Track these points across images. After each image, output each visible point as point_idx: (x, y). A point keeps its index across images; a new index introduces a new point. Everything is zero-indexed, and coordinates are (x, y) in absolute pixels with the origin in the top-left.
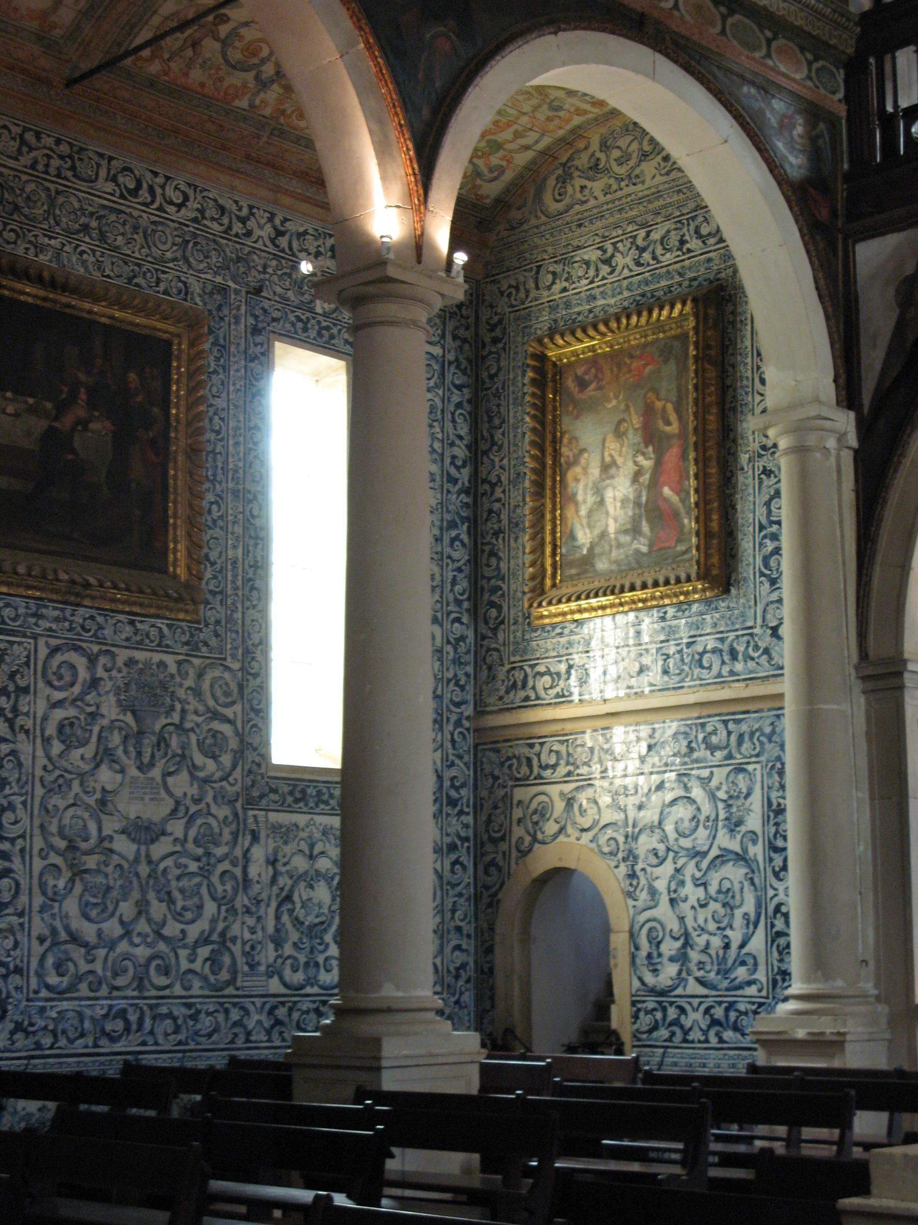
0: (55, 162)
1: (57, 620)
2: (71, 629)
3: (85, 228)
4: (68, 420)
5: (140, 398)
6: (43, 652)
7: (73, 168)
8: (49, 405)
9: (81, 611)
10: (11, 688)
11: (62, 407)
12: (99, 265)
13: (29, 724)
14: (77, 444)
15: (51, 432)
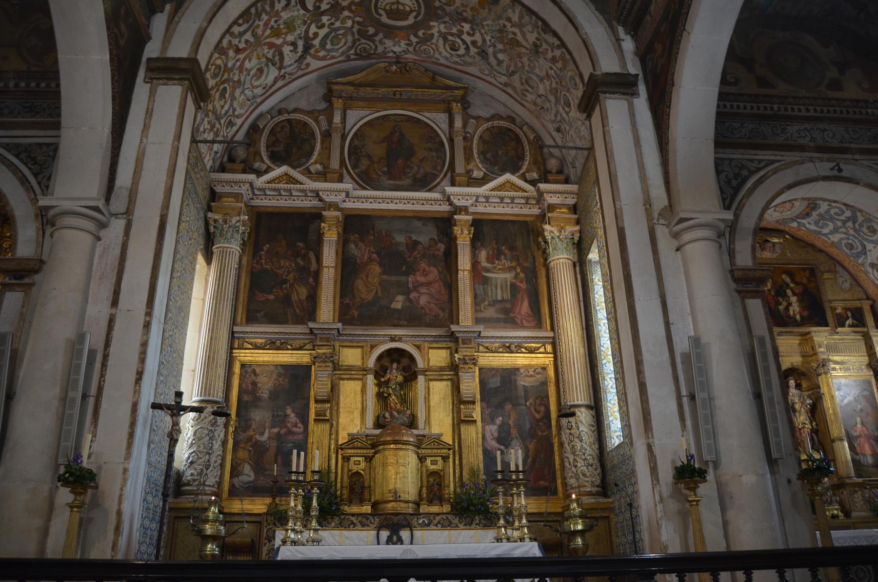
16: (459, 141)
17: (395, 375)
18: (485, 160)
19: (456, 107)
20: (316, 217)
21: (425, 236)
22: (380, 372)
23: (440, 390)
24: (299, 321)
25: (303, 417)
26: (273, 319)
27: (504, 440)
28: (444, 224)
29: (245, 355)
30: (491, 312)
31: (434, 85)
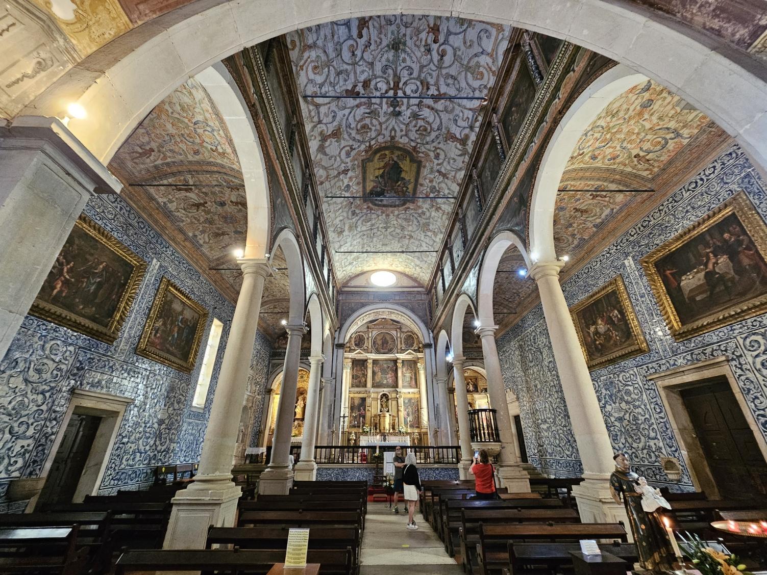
0: (670, 205)
1: (741, 328)
2: (748, 329)
3: (687, 212)
4: (710, 266)
5: (733, 239)
6: (741, 341)
7: (675, 201)
8: (702, 267)
9: (749, 321)
10: (735, 357)
11: (706, 265)
12: (697, 216)
13: (749, 367)
14: (717, 270)
15: (707, 273)
16: (399, 340)
17: (384, 399)
18: (405, 344)
19: (398, 330)
20: (366, 360)
21: (391, 364)
22: (382, 398)
23: (394, 403)
24: (363, 387)
25: (365, 410)
26: (357, 386)
27: (408, 415)
28: (395, 361)
29: (352, 395)
30: (406, 384)
31: (393, 324)
